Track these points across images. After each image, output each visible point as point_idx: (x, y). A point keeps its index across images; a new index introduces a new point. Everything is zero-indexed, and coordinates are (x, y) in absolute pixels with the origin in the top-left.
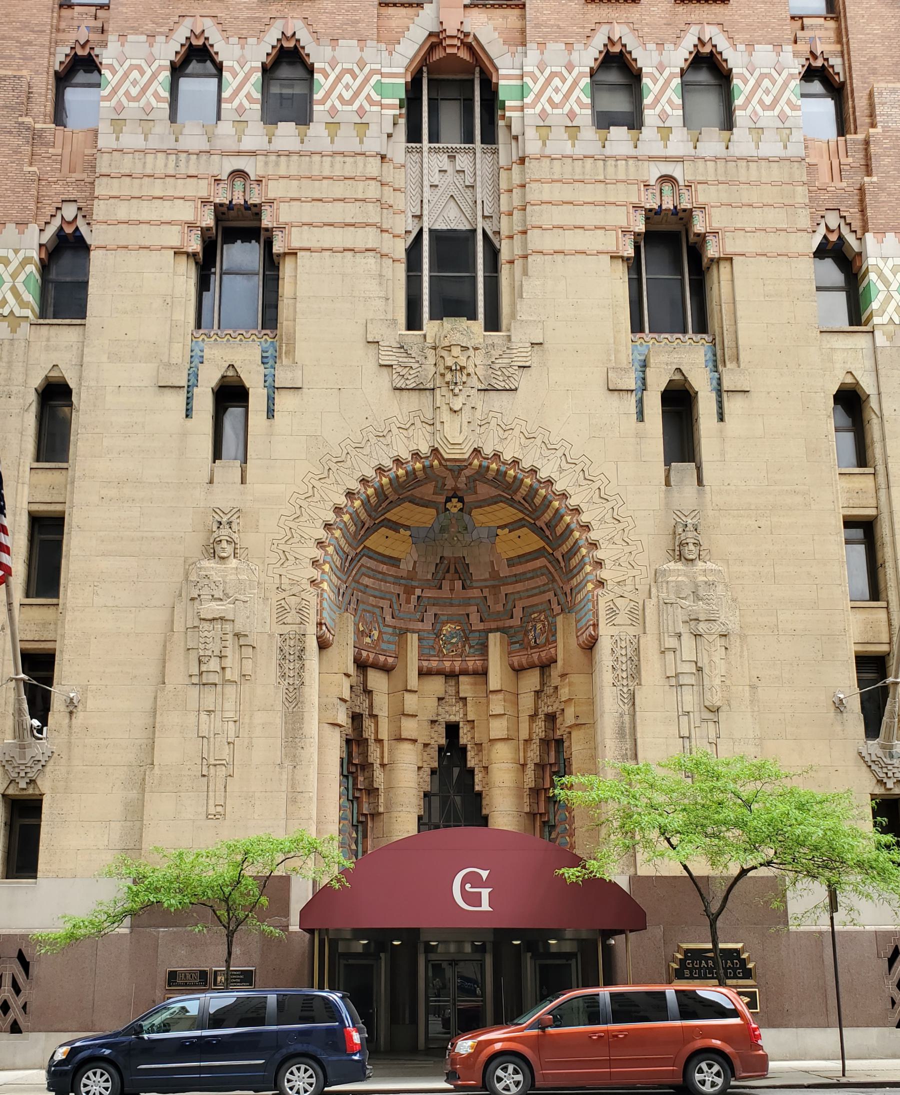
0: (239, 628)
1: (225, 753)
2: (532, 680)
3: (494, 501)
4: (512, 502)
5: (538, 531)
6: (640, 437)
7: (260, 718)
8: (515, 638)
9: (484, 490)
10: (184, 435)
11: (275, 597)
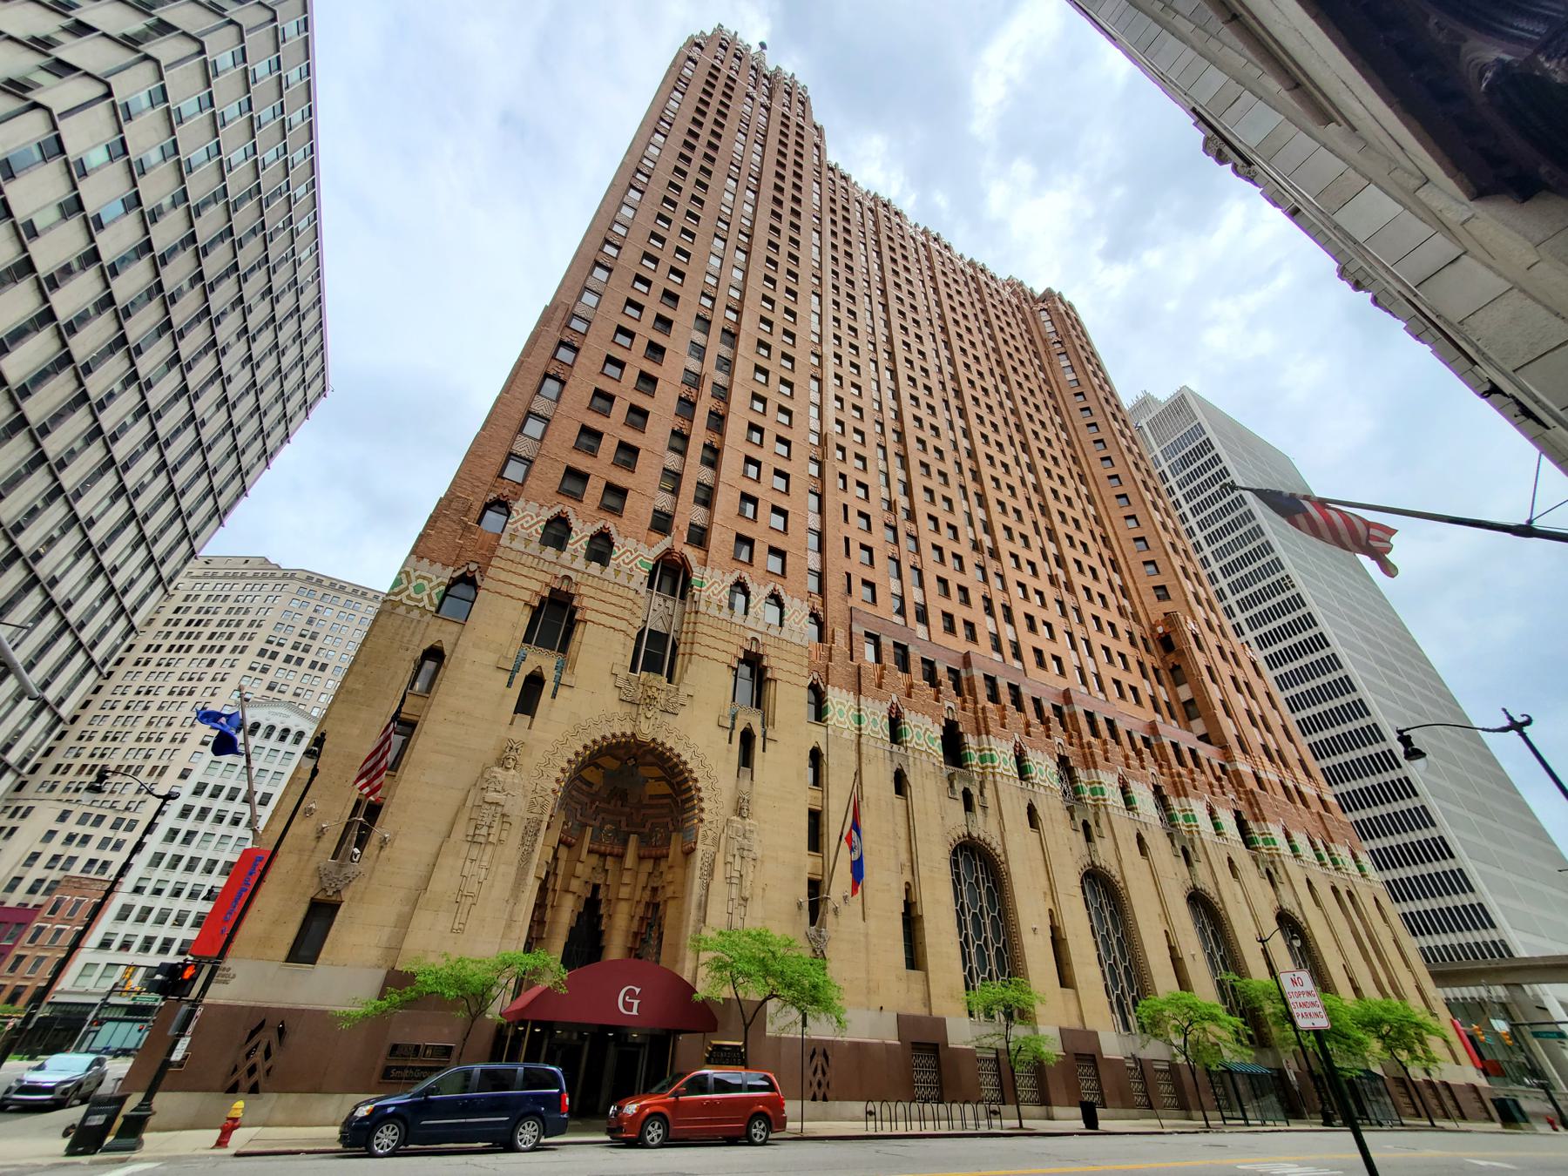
0: (505, 810)
1: (475, 889)
2: (648, 866)
3: (652, 764)
4: (661, 768)
5: (671, 785)
6: (729, 751)
7: (502, 868)
8: (644, 840)
9: (649, 758)
10: (504, 696)
11: (530, 796)
